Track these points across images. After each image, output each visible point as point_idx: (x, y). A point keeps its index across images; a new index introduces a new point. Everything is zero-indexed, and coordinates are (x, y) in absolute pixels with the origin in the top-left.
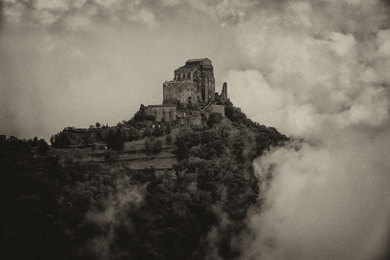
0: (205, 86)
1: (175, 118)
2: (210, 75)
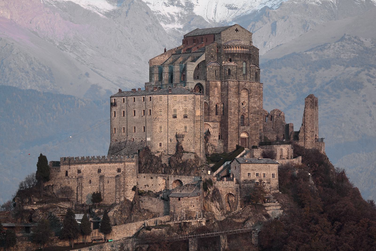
1: (131, 196)
2: (244, 72)
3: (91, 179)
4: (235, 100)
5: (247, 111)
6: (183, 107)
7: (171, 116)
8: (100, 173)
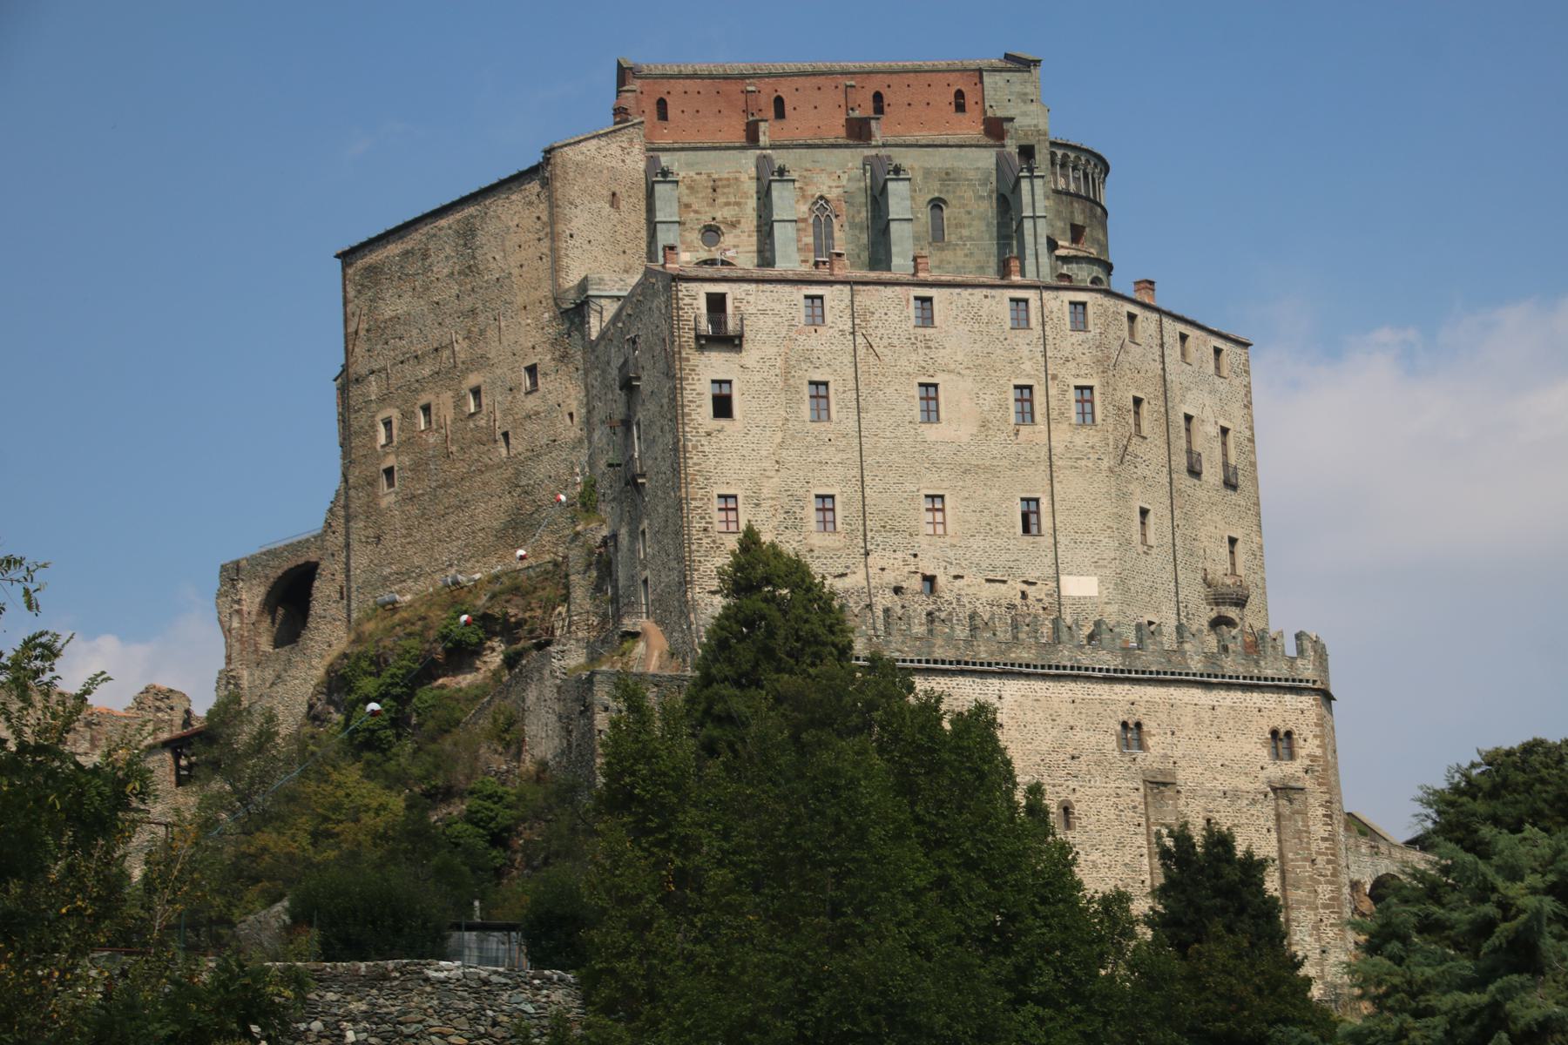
3: (1072, 798)
7: (1181, 461)
8: (1140, 755)
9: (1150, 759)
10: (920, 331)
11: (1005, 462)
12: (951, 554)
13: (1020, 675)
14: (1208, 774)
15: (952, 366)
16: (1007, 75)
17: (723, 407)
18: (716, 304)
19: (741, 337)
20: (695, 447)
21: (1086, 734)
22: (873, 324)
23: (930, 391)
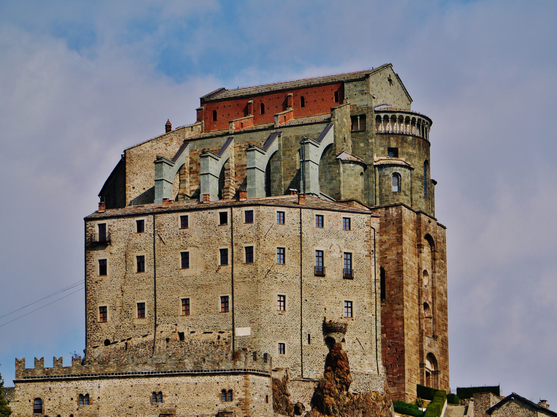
0: (400, 272)
4: (416, 260)
5: (430, 299)
6: (342, 247)
8: (160, 404)
9: (164, 406)
10: (182, 230)
11: (214, 283)
12: (191, 322)
13: (108, 378)
14: (190, 409)
15: (194, 244)
16: (355, 83)
17: (103, 271)
18: (102, 227)
19: (110, 241)
20: (91, 288)
21: (137, 398)
22: (163, 229)
23: (185, 256)
